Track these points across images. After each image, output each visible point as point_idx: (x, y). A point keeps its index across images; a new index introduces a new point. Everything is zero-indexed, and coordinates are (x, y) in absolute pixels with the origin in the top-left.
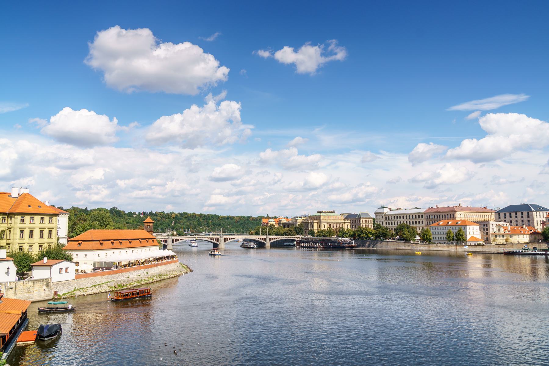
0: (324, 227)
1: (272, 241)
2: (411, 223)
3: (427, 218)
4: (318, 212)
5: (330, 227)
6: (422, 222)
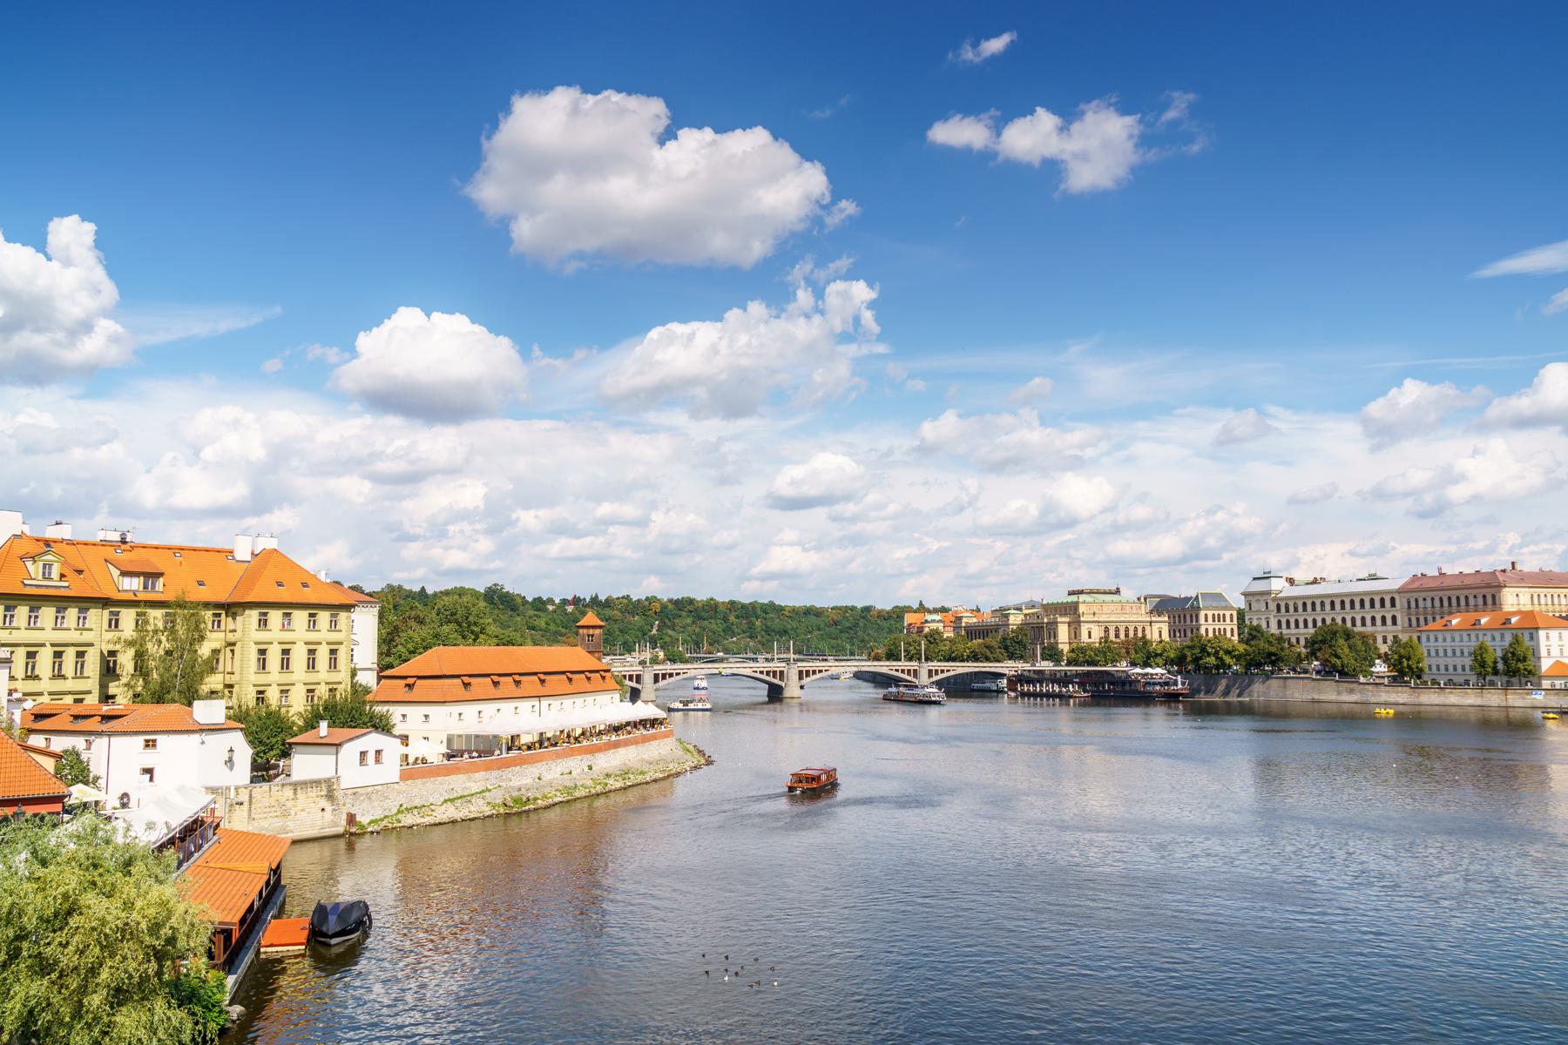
0: (1090, 637)
2: (1359, 623)
3: (1409, 607)
4: (1071, 593)
5: (1107, 637)
6: (1394, 618)
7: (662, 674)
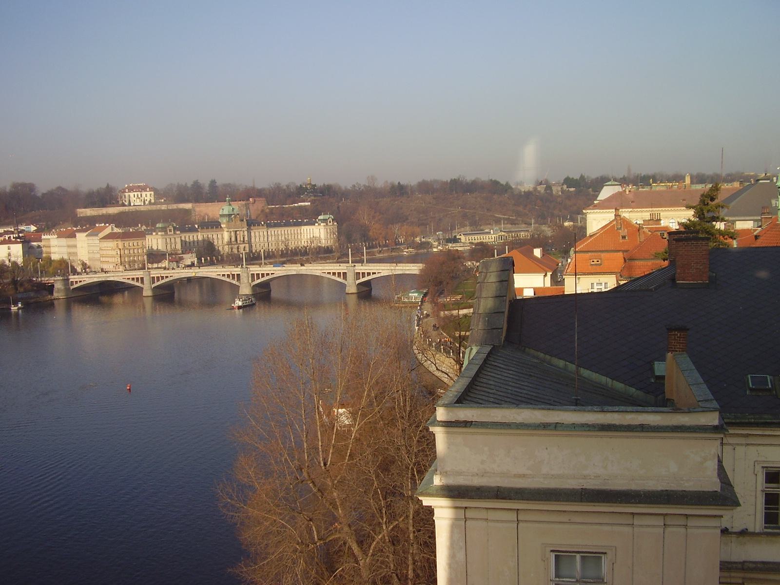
1: (362, 280)
7: (157, 277)
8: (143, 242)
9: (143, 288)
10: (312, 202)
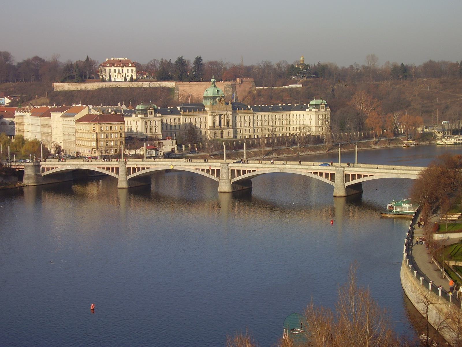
1: (352, 182)
7: (133, 168)
8: (121, 127)
9: (118, 179)
10: (304, 84)
